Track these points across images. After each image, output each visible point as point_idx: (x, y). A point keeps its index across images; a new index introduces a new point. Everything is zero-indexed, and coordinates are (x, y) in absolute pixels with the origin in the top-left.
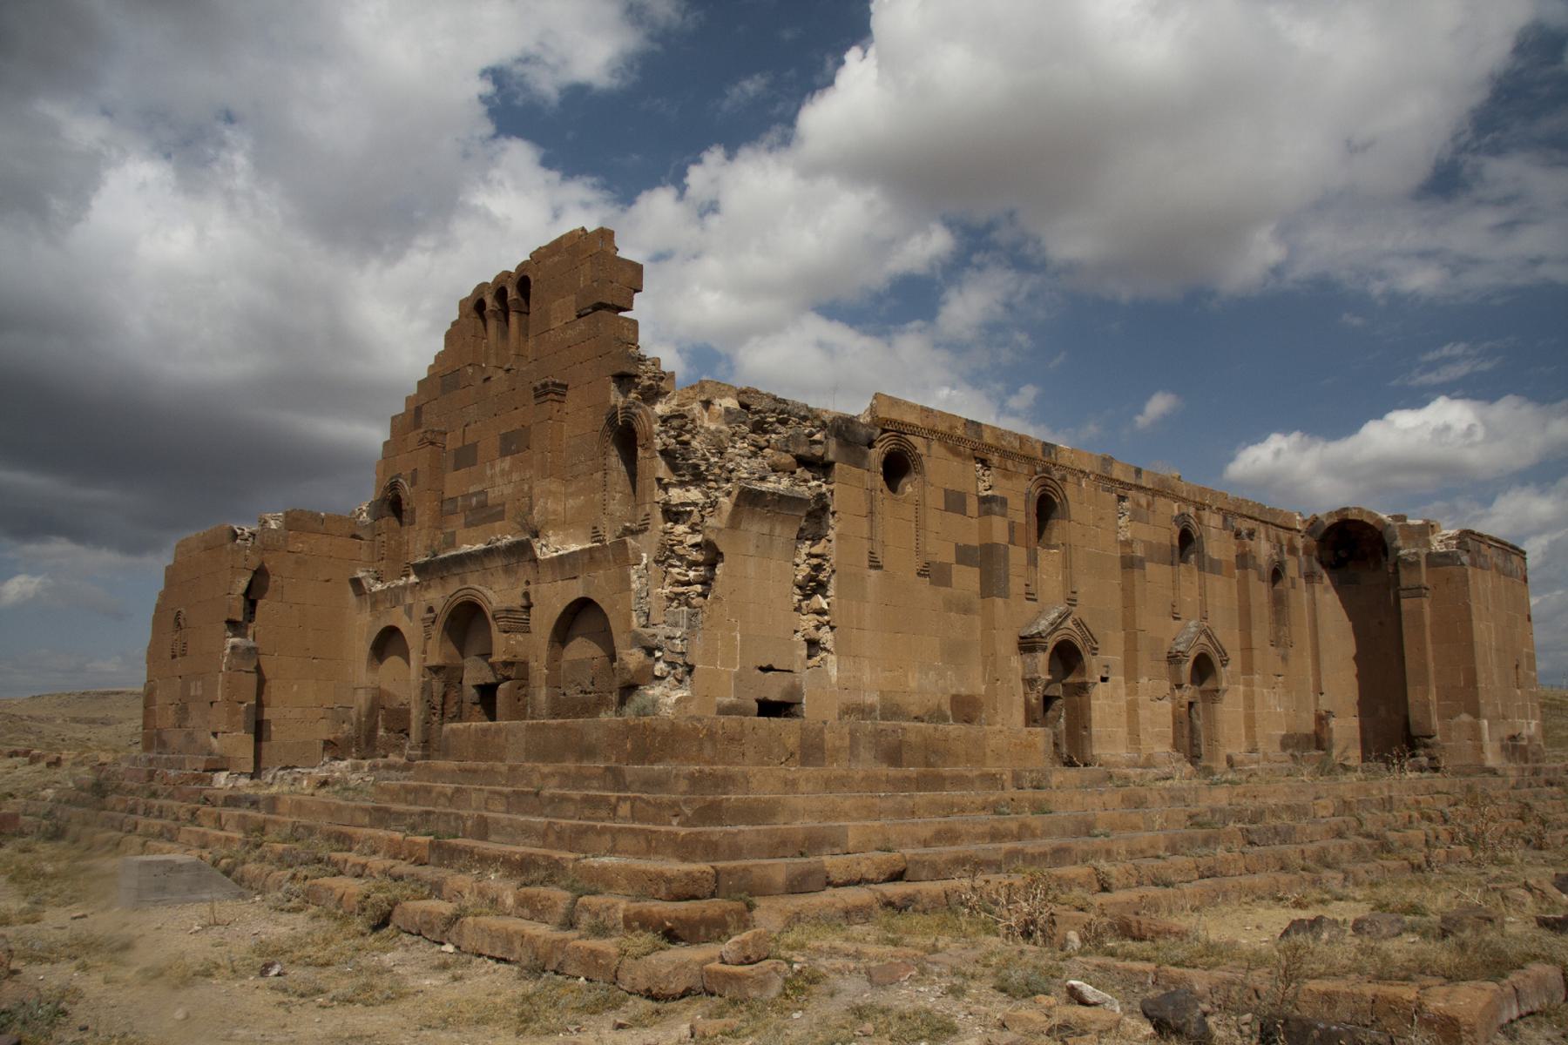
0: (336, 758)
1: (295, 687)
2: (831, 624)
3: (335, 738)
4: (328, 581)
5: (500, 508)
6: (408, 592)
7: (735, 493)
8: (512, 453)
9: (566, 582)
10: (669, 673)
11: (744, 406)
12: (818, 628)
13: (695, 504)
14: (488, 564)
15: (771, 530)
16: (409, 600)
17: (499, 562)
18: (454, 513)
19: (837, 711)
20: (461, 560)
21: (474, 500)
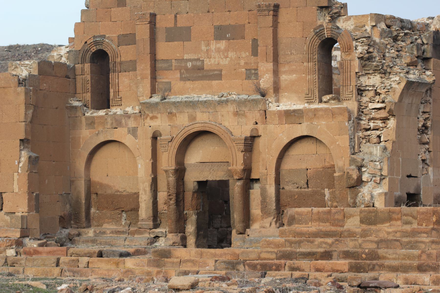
0: (64, 228)
1: (47, 181)
2: (430, 150)
3: (64, 214)
4: (57, 108)
5: (216, 72)
6: (132, 119)
7: (403, 84)
8: (229, 39)
9: (291, 125)
10: (371, 180)
11: (389, 27)
12: (425, 152)
13: (374, 86)
14: (219, 108)
15: (412, 101)
16: (132, 124)
17: (231, 108)
18: (169, 68)
19: (433, 198)
20: (192, 104)
21: (189, 65)
